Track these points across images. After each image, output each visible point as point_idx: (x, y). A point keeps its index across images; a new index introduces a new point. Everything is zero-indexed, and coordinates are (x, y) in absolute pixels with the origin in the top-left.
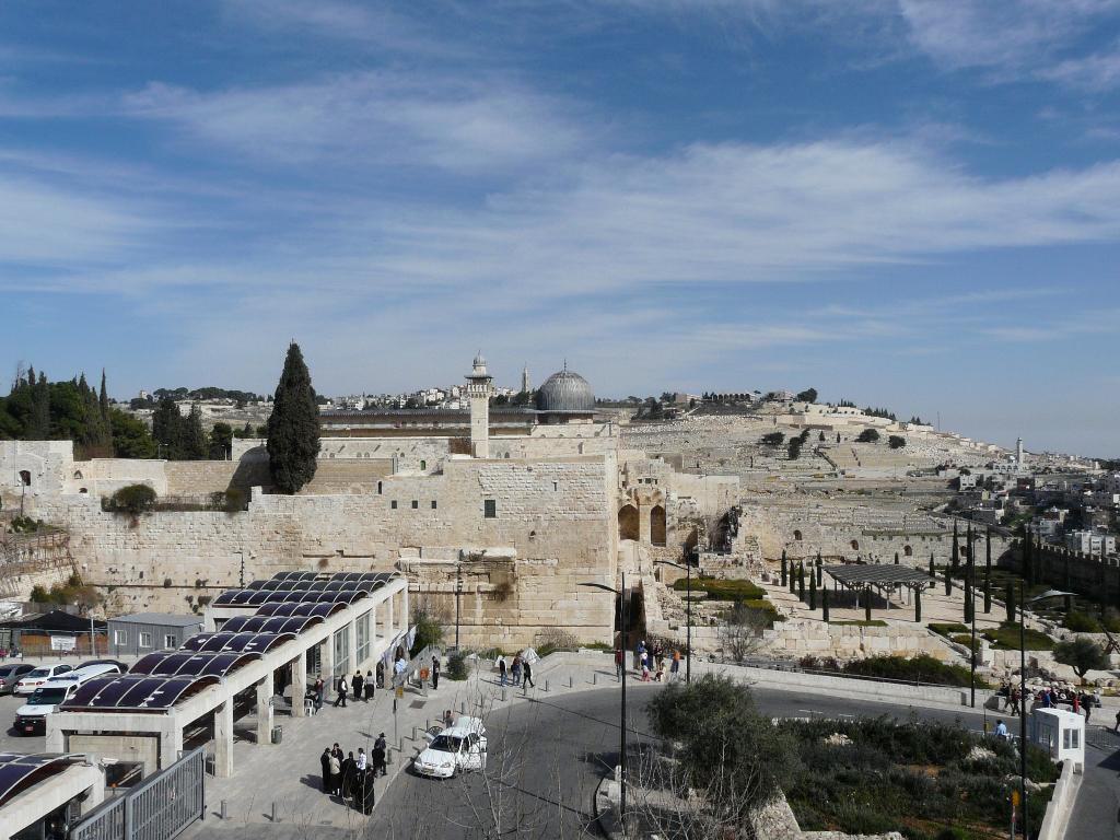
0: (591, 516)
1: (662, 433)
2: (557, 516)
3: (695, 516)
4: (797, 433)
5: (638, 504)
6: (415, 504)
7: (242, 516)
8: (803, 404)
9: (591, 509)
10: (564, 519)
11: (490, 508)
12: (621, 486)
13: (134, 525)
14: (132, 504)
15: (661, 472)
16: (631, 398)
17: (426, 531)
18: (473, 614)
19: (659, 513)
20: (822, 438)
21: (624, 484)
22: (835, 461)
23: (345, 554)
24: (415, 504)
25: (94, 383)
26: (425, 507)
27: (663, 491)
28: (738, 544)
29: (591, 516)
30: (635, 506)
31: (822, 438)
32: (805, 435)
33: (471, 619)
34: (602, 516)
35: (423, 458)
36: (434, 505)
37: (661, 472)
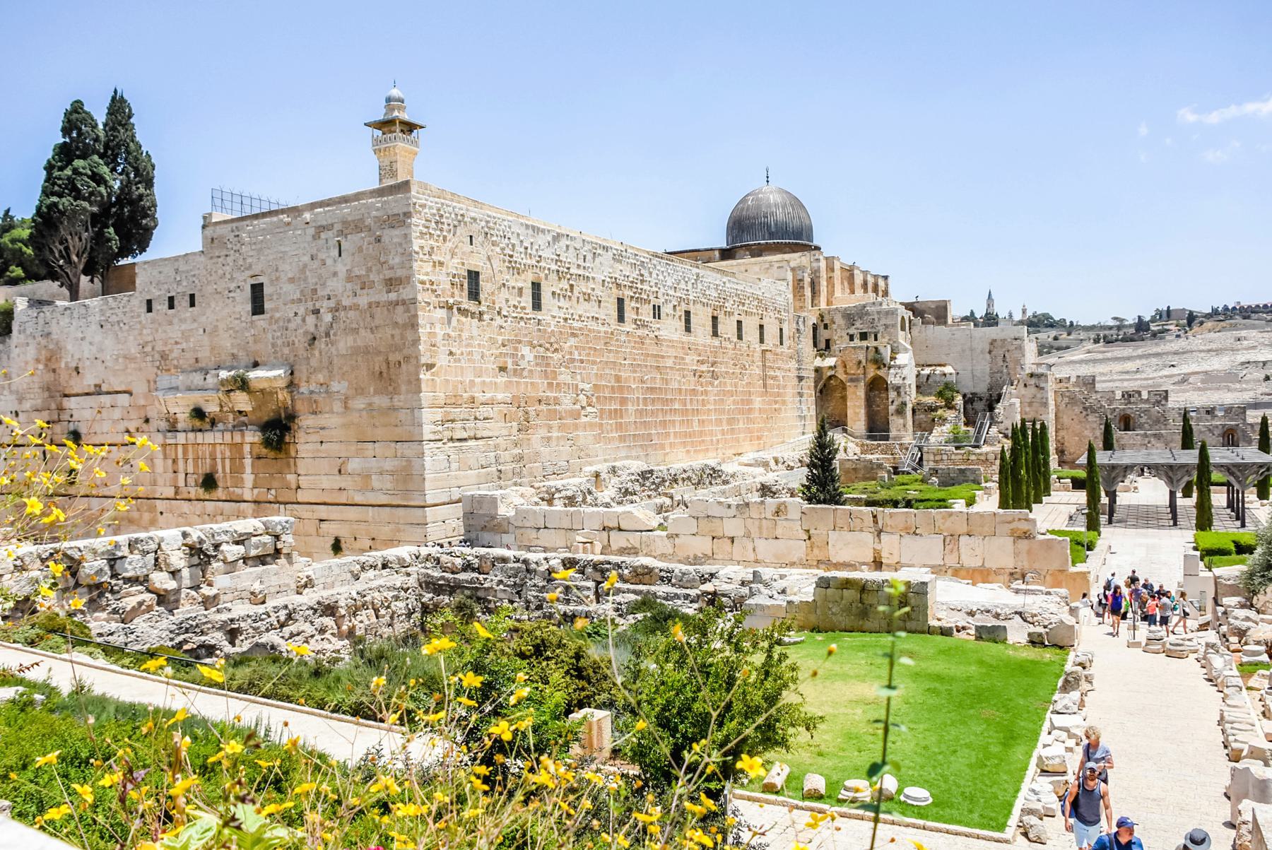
0: (393, 296)
1: (1140, 357)
2: (346, 302)
5: (846, 373)
6: (171, 303)
9: (391, 284)
10: (355, 307)
12: (823, 345)
15: (883, 321)
16: (1115, 318)
17: (184, 346)
18: (239, 483)
19: (877, 387)
21: (828, 341)
23: (104, 388)
24: (171, 303)
29: (393, 296)
30: (841, 376)
33: (238, 491)
34: (405, 293)
37: (883, 321)
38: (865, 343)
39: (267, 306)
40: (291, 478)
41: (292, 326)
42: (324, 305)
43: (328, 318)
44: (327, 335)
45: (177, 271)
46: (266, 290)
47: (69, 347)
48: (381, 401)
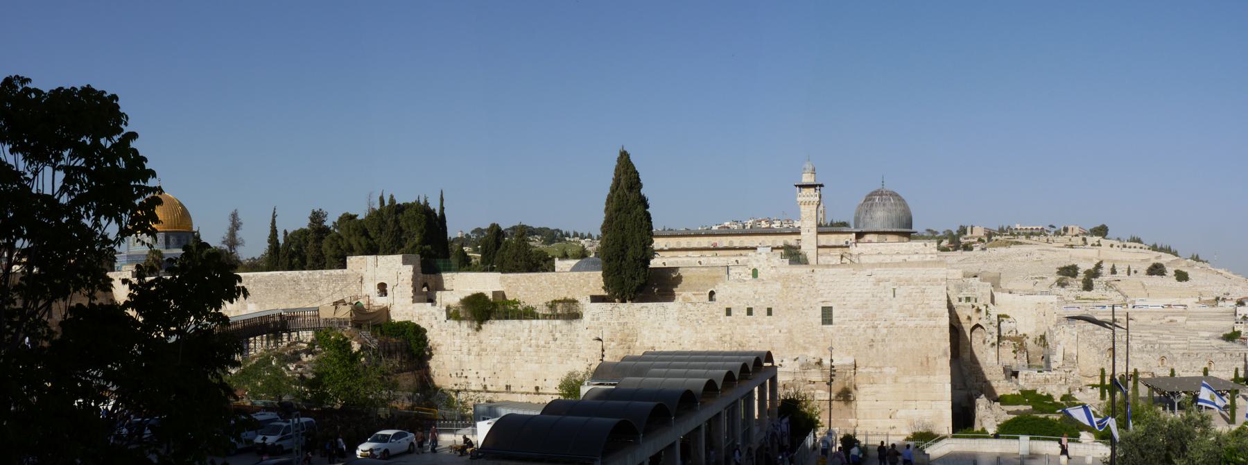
0: (932, 323)
3: (1013, 334)
4: (1091, 266)
6: (750, 312)
7: (575, 323)
8: (1096, 239)
10: (905, 327)
11: (827, 316)
13: (479, 329)
14: (480, 310)
20: (1114, 271)
22: (1126, 293)
24: (750, 312)
25: (434, 205)
26: (759, 314)
27: (983, 308)
28: (1057, 360)
29: (932, 323)
31: (1114, 271)
32: (1099, 266)
35: (755, 265)
36: (769, 312)
38: (969, 304)
39: (834, 320)
40: (852, 421)
41: (856, 333)
42: (882, 326)
43: (885, 331)
44: (883, 340)
45: (755, 292)
46: (835, 313)
47: (646, 332)
48: (924, 379)
